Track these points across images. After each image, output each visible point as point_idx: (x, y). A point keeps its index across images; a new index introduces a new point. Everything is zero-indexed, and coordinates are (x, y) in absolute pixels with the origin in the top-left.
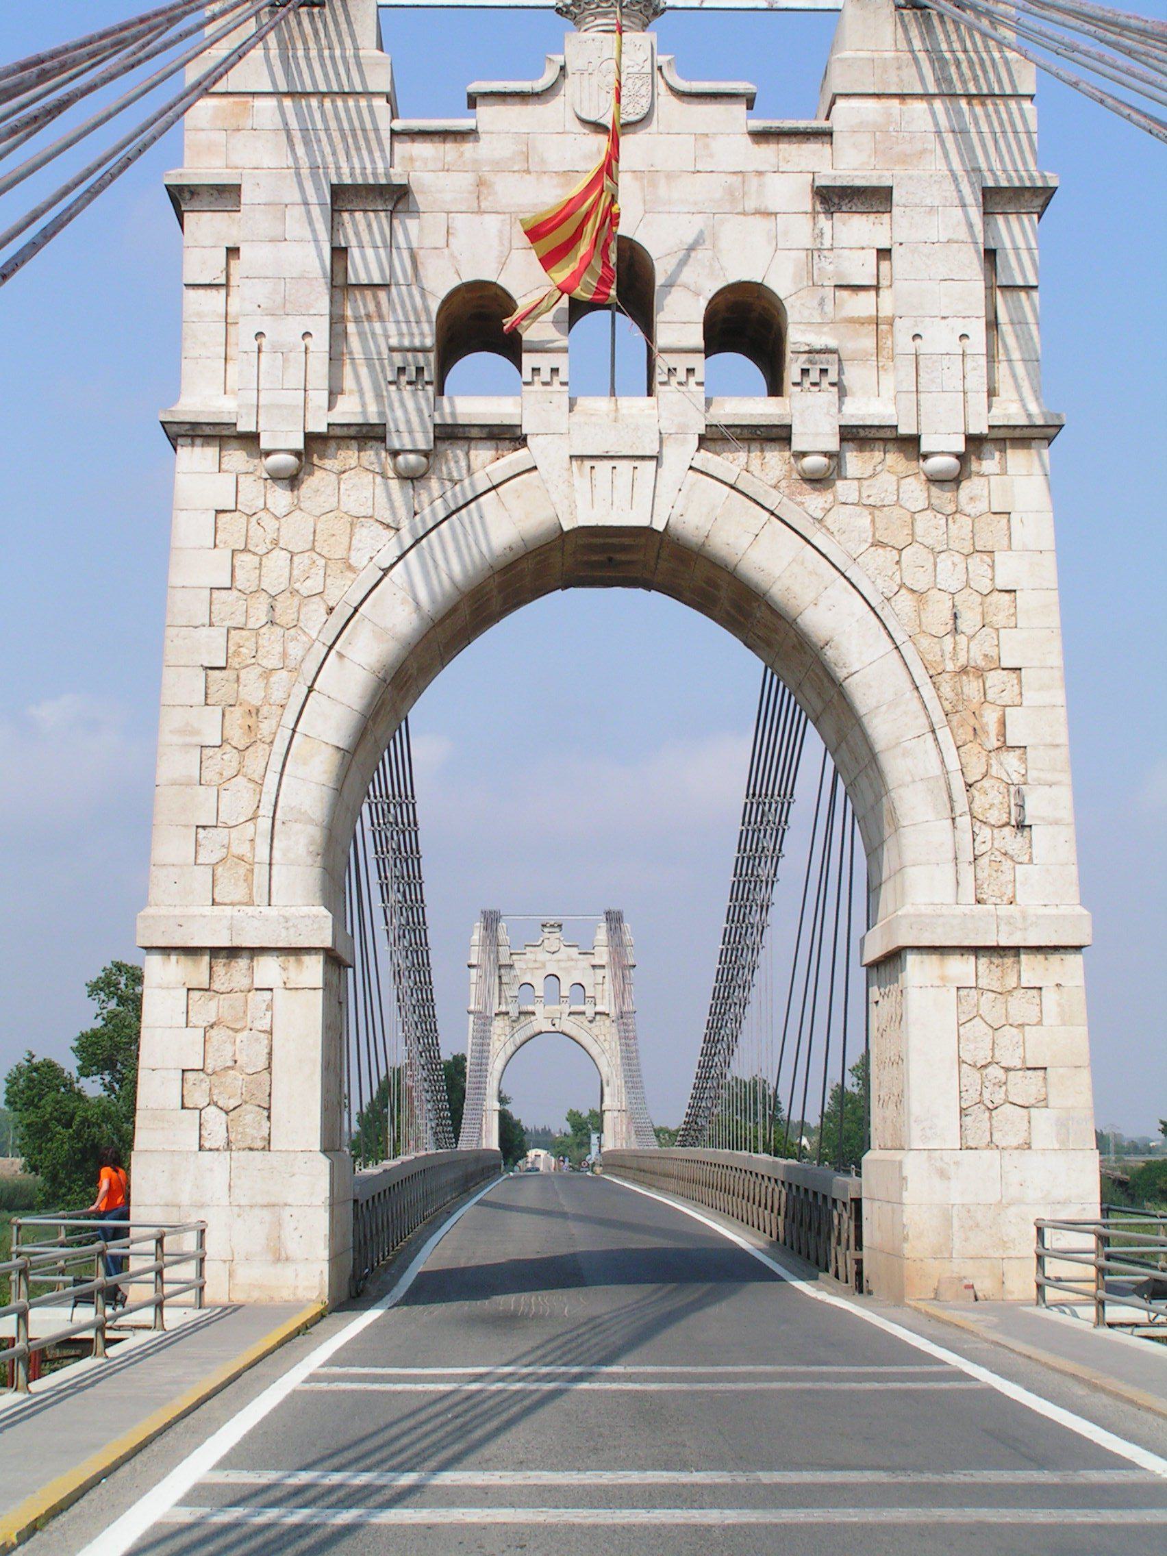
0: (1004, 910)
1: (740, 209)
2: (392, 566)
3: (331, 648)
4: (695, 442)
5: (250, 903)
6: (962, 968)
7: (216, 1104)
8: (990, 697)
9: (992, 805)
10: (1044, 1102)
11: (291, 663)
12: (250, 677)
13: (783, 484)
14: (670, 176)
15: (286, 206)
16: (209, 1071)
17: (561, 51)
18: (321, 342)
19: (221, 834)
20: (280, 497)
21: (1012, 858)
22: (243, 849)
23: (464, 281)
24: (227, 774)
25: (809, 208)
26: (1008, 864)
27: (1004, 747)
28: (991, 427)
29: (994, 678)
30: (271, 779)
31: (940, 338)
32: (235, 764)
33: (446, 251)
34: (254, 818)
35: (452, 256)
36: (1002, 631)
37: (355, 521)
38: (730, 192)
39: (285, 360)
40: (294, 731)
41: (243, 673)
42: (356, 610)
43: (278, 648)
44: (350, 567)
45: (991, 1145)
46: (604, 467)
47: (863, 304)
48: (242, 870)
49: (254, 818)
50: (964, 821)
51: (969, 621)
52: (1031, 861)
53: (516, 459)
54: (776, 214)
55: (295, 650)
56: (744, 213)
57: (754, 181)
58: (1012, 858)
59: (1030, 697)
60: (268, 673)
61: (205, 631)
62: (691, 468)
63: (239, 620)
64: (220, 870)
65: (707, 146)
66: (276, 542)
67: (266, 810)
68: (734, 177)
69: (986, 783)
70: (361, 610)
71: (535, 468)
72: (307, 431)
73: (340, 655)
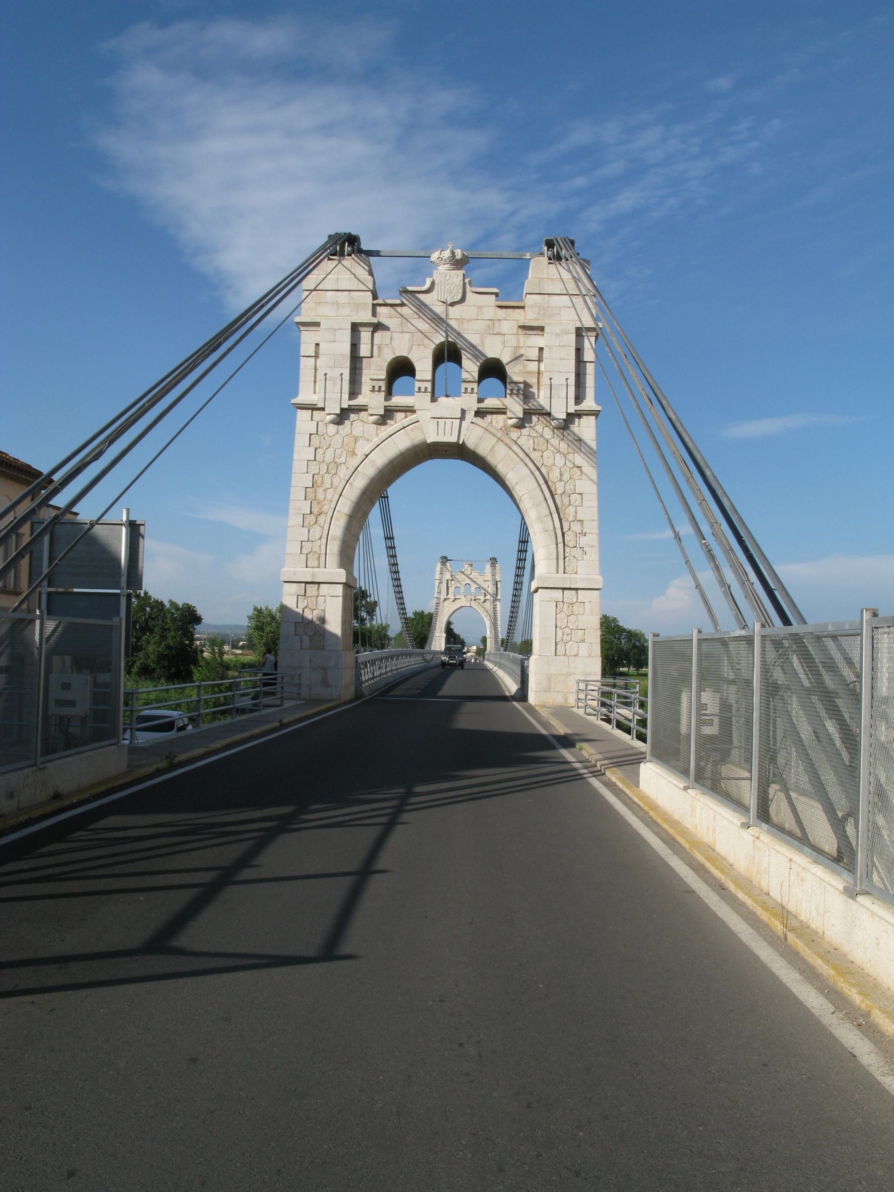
0: (574, 576)
1: (492, 333)
2: (369, 454)
3: (348, 481)
4: (473, 413)
5: (319, 567)
6: (558, 594)
7: (306, 634)
8: (572, 502)
9: (570, 540)
10: (583, 641)
11: (334, 486)
12: (320, 491)
13: (503, 428)
14: (469, 321)
15: (336, 330)
16: (304, 622)
17: (431, 276)
18: (346, 377)
19: (310, 544)
20: (332, 428)
21: (576, 558)
22: (317, 549)
23: (397, 356)
24: (312, 523)
25: (515, 332)
26: (575, 560)
27: (575, 520)
28: (575, 411)
29: (573, 497)
30: (327, 526)
31: (559, 380)
32: (315, 520)
33: (390, 346)
34: (320, 538)
35: (392, 347)
36: (576, 481)
37: (356, 440)
38: (489, 327)
39: (334, 383)
40: (335, 509)
41: (318, 489)
42: (356, 469)
43: (330, 481)
44: (355, 454)
45: (565, 655)
46: (441, 421)
47: (533, 366)
48: (316, 556)
49: (320, 538)
50: (561, 545)
51: (566, 477)
52: (583, 559)
53: (412, 417)
54: (504, 335)
55: (336, 481)
56: (493, 334)
57: (497, 323)
58: (576, 558)
59: (585, 503)
60: (325, 490)
61: (306, 475)
62: (472, 423)
63: (317, 472)
64: (308, 557)
65: (481, 311)
66: (330, 445)
67: (325, 536)
68: (489, 322)
69: (569, 532)
70: (358, 469)
71: (418, 421)
72: (342, 407)
73: (351, 484)
